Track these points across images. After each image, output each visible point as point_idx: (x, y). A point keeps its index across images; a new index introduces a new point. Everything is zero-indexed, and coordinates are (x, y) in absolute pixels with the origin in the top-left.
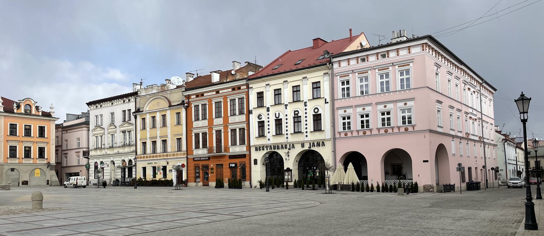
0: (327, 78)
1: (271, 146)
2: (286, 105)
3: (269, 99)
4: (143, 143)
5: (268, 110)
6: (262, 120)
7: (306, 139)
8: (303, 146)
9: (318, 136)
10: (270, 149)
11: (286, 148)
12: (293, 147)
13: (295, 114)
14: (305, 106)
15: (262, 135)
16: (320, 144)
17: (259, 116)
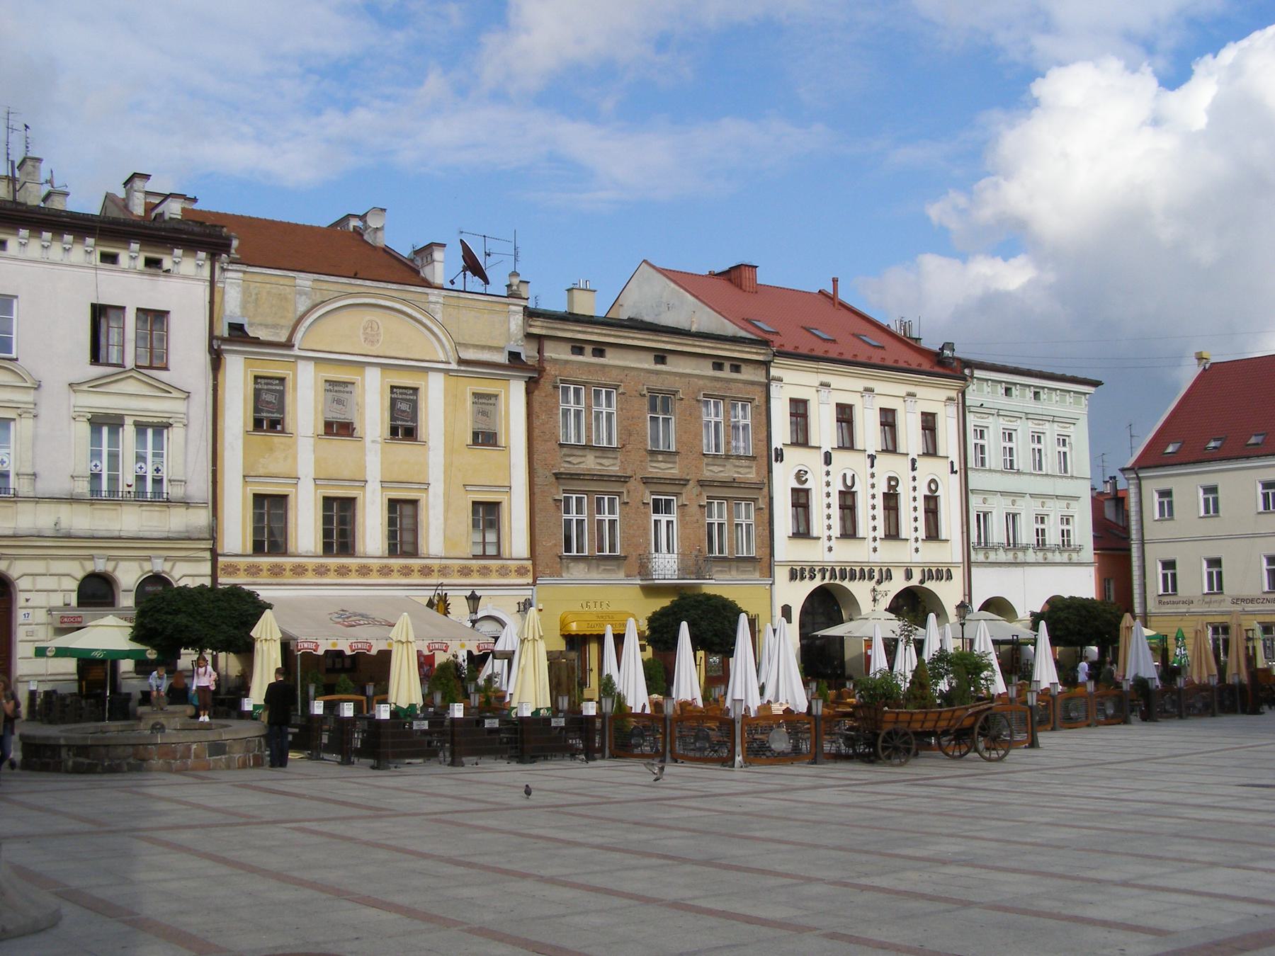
0: (952, 410)
1: (833, 570)
2: (872, 458)
3: (824, 428)
4: (259, 499)
5: (828, 459)
6: (806, 486)
7: (917, 558)
8: (909, 575)
9: (932, 554)
10: (831, 579)
11: (871, 578)
12: (889, 577)
13: (890, 487)
14: (914, 469)
15: (802, 532)
16: (942, 574)
17: (800, 476)
